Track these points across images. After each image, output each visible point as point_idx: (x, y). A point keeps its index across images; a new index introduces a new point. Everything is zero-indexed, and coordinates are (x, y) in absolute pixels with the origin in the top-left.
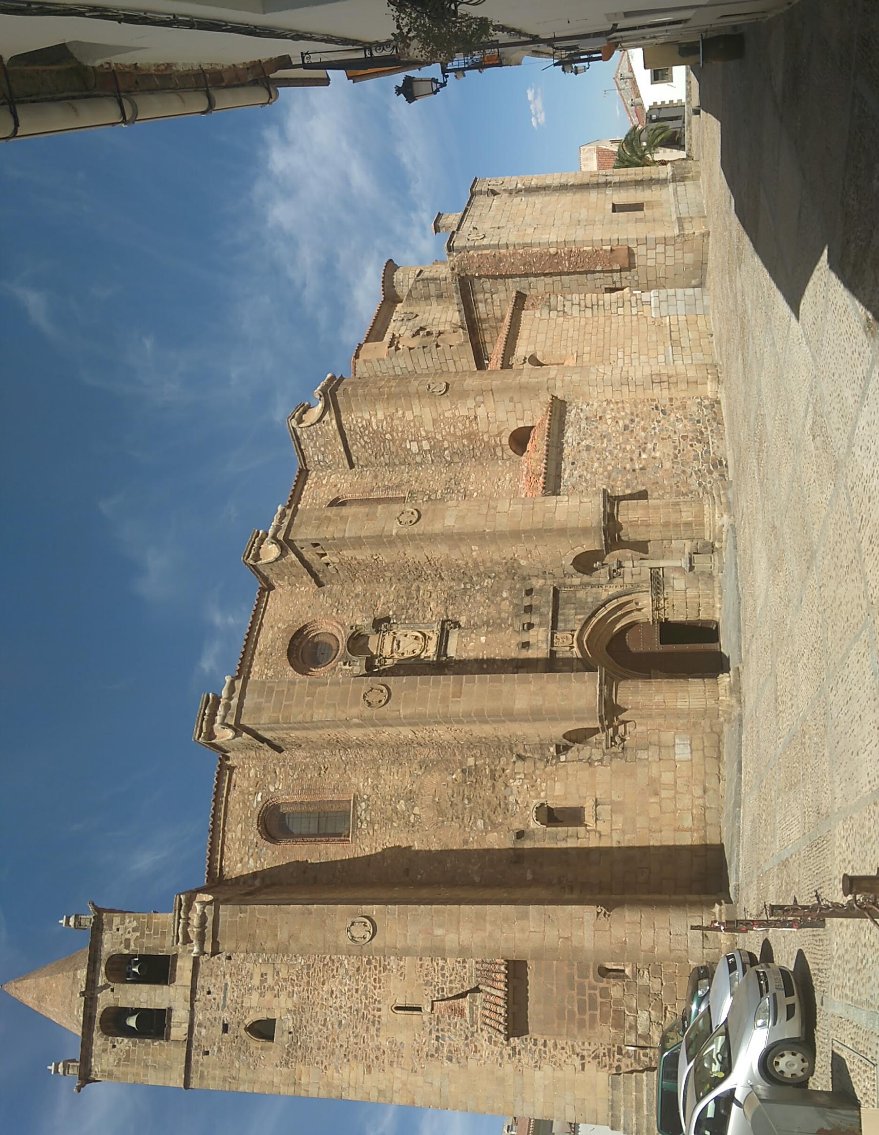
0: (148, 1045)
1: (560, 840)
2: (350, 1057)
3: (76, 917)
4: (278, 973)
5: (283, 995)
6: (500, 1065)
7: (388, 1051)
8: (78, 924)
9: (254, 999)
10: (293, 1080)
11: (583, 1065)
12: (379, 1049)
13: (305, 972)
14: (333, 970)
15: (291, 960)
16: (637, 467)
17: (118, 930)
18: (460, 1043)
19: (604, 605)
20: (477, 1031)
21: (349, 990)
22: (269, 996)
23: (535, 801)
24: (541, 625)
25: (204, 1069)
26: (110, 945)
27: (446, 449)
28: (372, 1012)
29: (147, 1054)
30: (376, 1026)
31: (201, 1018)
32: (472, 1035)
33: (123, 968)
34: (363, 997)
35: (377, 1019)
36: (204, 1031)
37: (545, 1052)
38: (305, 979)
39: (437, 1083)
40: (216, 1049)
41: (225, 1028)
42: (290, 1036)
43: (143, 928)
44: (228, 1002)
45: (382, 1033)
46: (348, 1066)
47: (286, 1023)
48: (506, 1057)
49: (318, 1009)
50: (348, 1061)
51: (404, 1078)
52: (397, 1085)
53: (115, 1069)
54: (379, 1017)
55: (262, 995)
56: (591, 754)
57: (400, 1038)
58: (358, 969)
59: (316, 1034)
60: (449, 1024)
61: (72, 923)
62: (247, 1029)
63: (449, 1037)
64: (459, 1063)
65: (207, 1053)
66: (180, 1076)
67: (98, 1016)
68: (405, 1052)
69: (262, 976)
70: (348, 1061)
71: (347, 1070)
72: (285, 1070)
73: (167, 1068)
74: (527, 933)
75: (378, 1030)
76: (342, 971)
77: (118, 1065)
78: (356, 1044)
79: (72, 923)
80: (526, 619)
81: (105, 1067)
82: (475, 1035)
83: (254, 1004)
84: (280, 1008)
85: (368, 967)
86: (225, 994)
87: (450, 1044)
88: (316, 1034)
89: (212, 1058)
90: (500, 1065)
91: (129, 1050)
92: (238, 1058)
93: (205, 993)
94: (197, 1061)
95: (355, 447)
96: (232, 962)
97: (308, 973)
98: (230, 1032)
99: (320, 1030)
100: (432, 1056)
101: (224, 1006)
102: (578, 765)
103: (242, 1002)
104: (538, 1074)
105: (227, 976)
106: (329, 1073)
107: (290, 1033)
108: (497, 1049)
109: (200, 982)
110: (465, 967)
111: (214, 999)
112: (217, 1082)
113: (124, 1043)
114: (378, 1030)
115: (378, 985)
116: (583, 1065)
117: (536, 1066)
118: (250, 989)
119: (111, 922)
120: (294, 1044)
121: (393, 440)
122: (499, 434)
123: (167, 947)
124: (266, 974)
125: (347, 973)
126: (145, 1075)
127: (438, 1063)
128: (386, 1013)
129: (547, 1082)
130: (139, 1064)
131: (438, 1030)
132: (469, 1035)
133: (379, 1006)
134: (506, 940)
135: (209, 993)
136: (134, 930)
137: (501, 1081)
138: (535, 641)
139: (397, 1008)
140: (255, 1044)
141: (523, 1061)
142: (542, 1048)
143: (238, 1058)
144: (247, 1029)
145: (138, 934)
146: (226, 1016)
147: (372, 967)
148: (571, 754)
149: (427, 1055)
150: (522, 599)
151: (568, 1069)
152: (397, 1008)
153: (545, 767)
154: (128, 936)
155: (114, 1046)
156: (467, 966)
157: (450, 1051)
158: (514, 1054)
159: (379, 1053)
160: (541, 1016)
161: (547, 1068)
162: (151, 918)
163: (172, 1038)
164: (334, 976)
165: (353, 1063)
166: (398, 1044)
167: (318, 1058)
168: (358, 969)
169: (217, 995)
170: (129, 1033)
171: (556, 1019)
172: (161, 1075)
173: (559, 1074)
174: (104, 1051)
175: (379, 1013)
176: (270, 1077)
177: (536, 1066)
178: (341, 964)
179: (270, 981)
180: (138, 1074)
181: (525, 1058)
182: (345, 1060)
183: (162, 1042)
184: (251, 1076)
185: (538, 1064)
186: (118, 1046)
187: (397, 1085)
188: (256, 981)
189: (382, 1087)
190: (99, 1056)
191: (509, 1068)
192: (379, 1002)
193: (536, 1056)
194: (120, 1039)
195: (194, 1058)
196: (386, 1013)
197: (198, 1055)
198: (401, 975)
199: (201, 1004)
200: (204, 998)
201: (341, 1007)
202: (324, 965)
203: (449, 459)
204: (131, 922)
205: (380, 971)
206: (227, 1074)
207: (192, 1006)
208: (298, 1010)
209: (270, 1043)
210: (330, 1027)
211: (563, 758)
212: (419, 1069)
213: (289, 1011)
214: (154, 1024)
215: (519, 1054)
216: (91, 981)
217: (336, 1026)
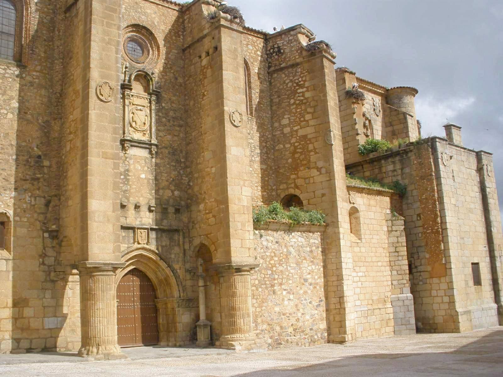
16: (275, 288)
19: (169, 266)
27: (284, 146)
56: (49, 257)
95: (283, 76)
102: (40, 246)
121: (290, 105)
122: (297, 187)
148: (48, 241)
153: (40, 221)
203: (277, 148)
211: (46, 235)
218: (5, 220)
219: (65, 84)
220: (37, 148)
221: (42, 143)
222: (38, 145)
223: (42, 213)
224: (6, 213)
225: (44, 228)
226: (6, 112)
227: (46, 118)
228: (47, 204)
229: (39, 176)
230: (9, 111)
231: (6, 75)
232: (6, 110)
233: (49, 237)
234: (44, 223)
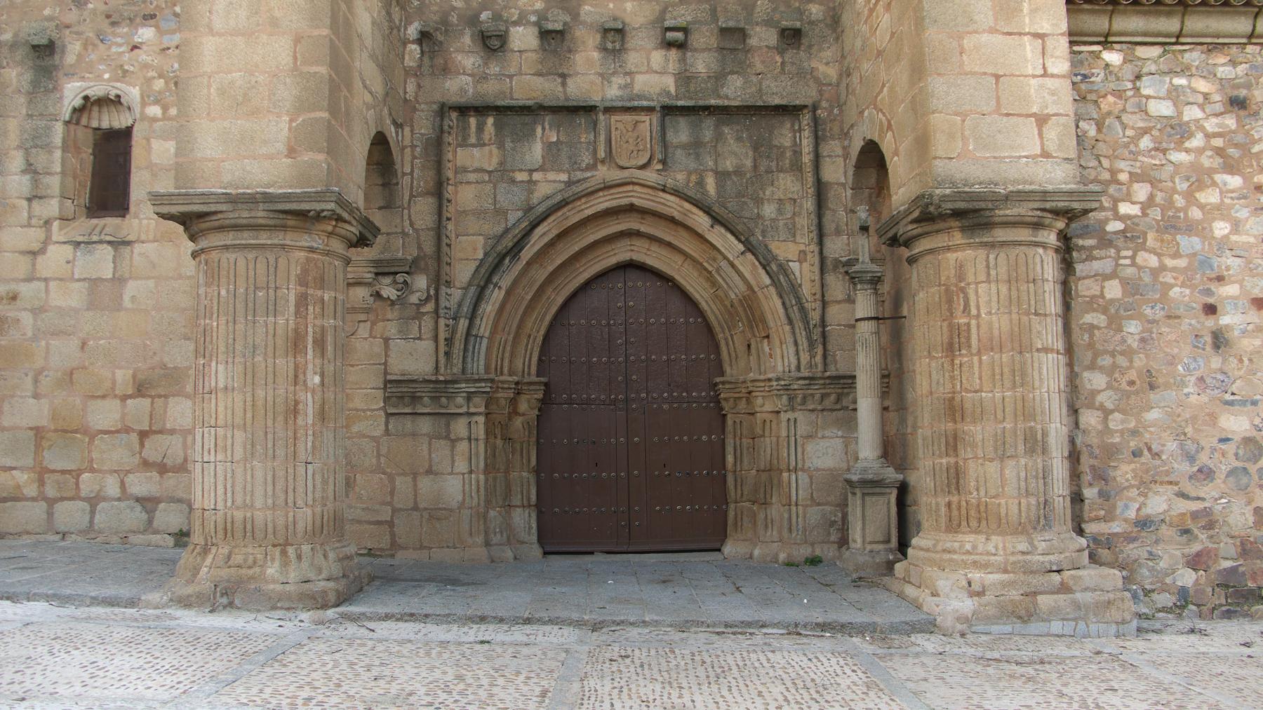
24: (684, 78)
80: (704, 38)
138: (630, 66)
150: (768, 23)
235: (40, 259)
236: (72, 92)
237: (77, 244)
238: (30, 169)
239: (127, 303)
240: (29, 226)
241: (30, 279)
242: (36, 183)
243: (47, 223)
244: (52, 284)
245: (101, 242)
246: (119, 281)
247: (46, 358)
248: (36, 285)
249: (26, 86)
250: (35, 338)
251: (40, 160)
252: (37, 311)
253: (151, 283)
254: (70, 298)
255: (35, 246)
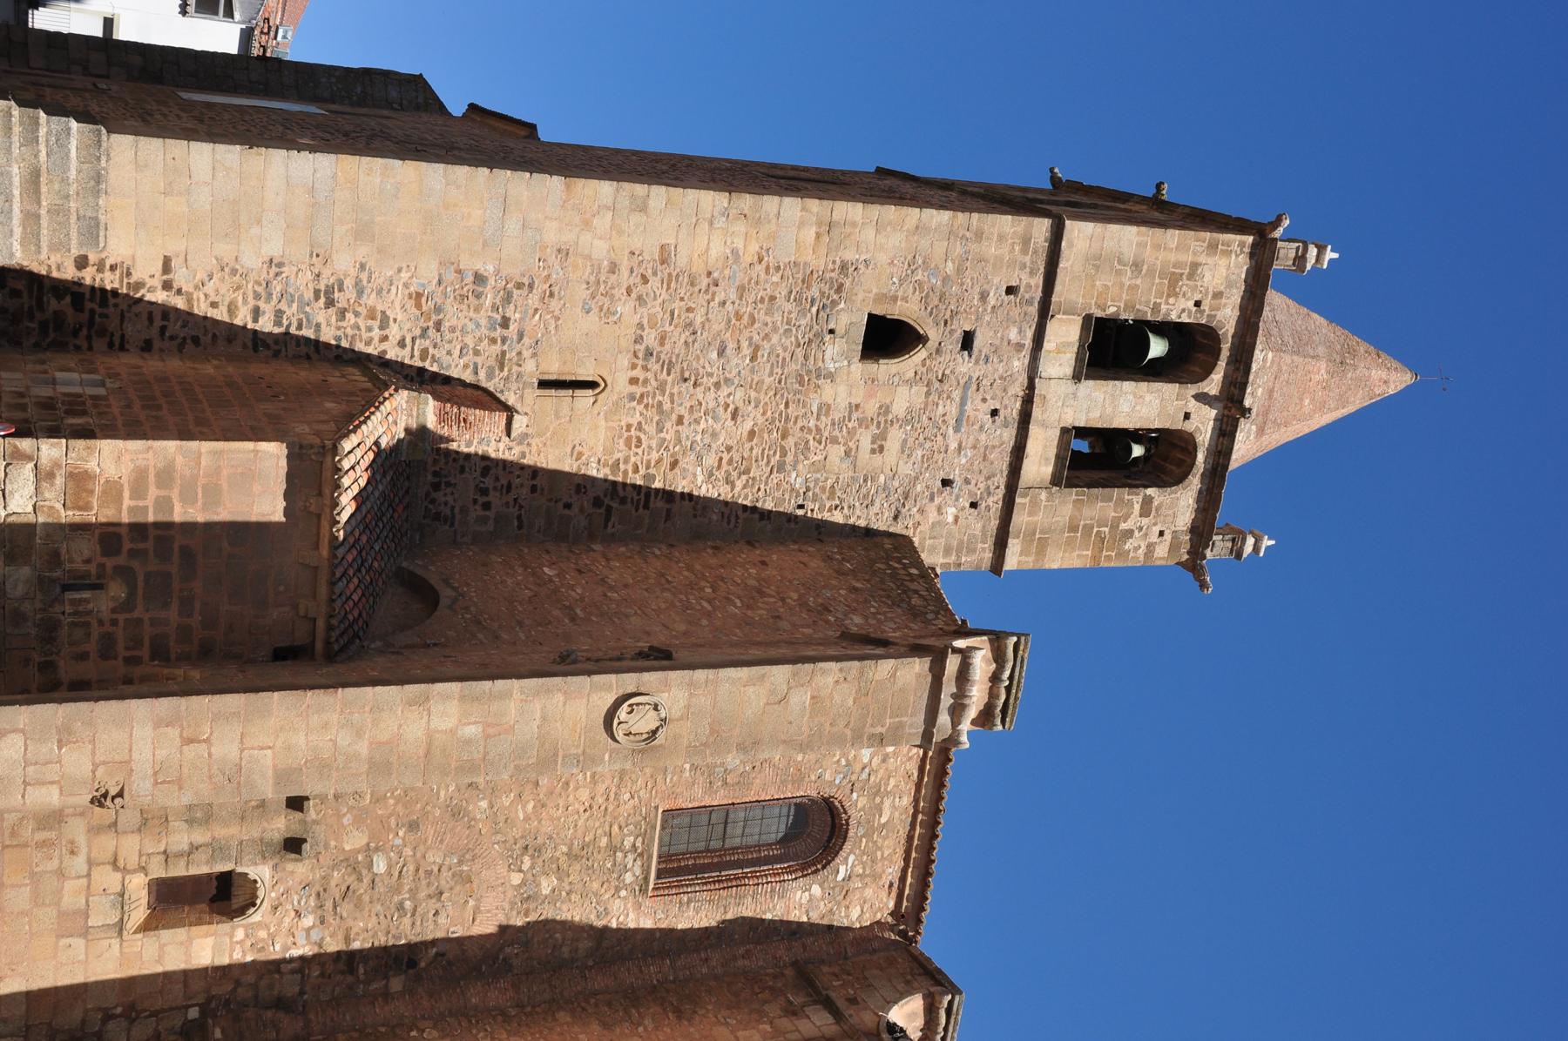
0: (1129, 306)
1: (206, 845)
2: (705, 281)
3: (1239, 555)
4: (847, 453)
5: (842, 403)
6: (362, 267)
7: (620, 292)
8: (1237, 539)
9: (903, 400)
10: (835, 232)
11: (167, 266)
12: (640, 298)
13: (789, 458)
14: (730, 462)
15: (816, 481)
17: (1161, 533)
18: (454, 315)
20: (414, 340)
21: (697, 422)
22: (871, 408)
23: (257, 918)
25: (1021, 258)
26: (1179, 505)
28: (650, 375)
29: (1133, 288)
30: (642, 347)
31: (1016, 363)
32: (425, 330)
33: (1163, 457)
34: (667, 406)
35: (640, 362)
36: (1013, 334)
37: (257, 296)
38: (790, 442)
39: (513, 225)
40: (992, 301)
41: (967, 341)
42: (831, 326)
43: (1113, 537)
44: (956, 395)
45: (631, 332)
46: (712, 260)
47: (841, 353)
48: (349, 283)
49: (768, 380)
50: (709, 274)
51: (586, 238)
52: (603, 222)
53: (1202, 259)
54: (634, 366)
55: (885, 409)
56: (129, 1030)
57: (591, 322)
58: (674, 464)
59: (775, 329)
60: (477, 353)
61: (1250, 541)
62: (921, 339)
63: (478, 326)
64: (459, 272)
65: (1010, 290)
66: (1071, 245)
67: (1222, 364)
68: (582, 293)
69: (881, 449)
70: (709, 274)
71: (713, 253)
72: (850, 255)
73: (1097, 261)
74: (279, 743)
75: (639, 340)
76: (710, 460)
77: (1195, 266)
78: (689, 310)
79: (1250, 541)
81: (1223, 262)
82: (418, 332)
83: (903, 391)
84: (850, 379)
85: (652, 471)
86: (962, 412)
87: (477, 310)
88: (775, 329)
89: (1000, 282)
90: (362, 267)
91: (1169, 296)
92: (946, 279)
93: (1002, 413)
94: (1032, 273)
96: (942, 475)
97: (784, 454)
98: (959, 335)
99: (767, 337)
100: (519, 286)
101: (966, 387)
103: (928, 394)
104: (274, 248)
105: (953, 445)
106: (754, 248)
107: (832, 332)
108: (370, 300)
109: (1009, 436)
110: (435, 474)
111: (984, 400)
112: (995, 231)
113: (1179, 310)
114: (639, 340)
115: (633, 432)
116: (167, 266)
117: (280, 265)
118: (907, 422)
119: (1174, 547)
120: (827, 307)
123: (1067, 506)
124: (873, 451)
125: (699, 457)
126: (1140, 245)
127: (507, 270)
128: (619, 383)
129: (255, 230)
130: (1151, 272)
131: (504, 340)
132: (432, 332)
133: (634, 389)
134: (325, 726)
135: (994, 413)
136: (1129, 534)
137: (362, 233)
139: (591, 385)
140: (906, 309)
141: (309, 276)
142: (261, 304)
143: (946, 279)
144: (921, 339)
145: (1123, 526)
146: (964, 366)
147: (642, 471)
149: (531, 286)
151: (203, 262)
152: (591, 385)
153: (234, 990)
154: (1145, 521)
155: (1198, 304)
156: (429, 477)
157: (478, 296)
158: (329, 291)
159: (641, 289)
160: (257, 488)
161: (252, 261)
162: (1094, 557)
163: (1079, 321)
164: (729, 449)
165: (699, 268)
166: (595, 310)
167: (776, 279)
168: (674, 464)
169: (978, 410)
170: (1165, 329)
171: (225, 486)
172: (1109, 244)
173: (225, 250)
174: (1218, 295)
175: (635, 373)
176: (881, 239)
177: (280, 265)
178: (711, 475)
179: (865, 439)
180: (1157, 247)
181: (303, 283)
182: (715, 275)
183: (1099, 314)
184: (924, 243)
185: (274, 269)
186: (1191, 303)
187: (603, 222)
188: (895, 436)
189: (636, 218)
190: (1230, 285)
191: (343, 264)
192: (632, 397)
193: (277, 288)
194: (1185, 319)
195: (1038, 280)
196: (619, 383)
197: (1029, 286)
198: (580, 454)
199: (1011, 391)
200: (1006, 401)
201: (717, 385)
202: (747, 472)
204: (1135, 550)
205: (626, 461)
206: (974, 247)
207: (1031, 386)
208: (813, 376)
209: (878, 311)
210: (745, 344)
211: (193, 1013)
212: (552, 260)
213: (831, 376)
214: (1112, 348)
215: (317, 293)
216: (1225, 433)
217: (731, 346)
218: (236, 903)
219: (609, 1004)
220: (437, 954)
221: (450, 963)
222: (443, 955)
223: (256, 997)
224: (254, 905)
225: (213, 1005)
226: (525, 867)
227: (515, 962)
228: (280, 1004)
229: (361, 971)
230: (529, 876)
231: (619, 855)
232: (533, 867)
233: (186, 1022)
234: (228, 1002)
235: (109, 868)
236: (262, 872)
237: (122, 895)
238: (194, 848)
239: (64, 942)
240: (141, 855)
241: (91, 863)
242: (180, 855)
243: (143, 869)
244: (84, 881)
245: (123, 913)
246: (85, 933)
247: (13, 886)
248: (84, 869)
249: (268, 836)
250: (33, 875)
251: (201, 856)
252: (61, 874)
253: (82, 957)
254: (72, 896)
255: (121, 864)
